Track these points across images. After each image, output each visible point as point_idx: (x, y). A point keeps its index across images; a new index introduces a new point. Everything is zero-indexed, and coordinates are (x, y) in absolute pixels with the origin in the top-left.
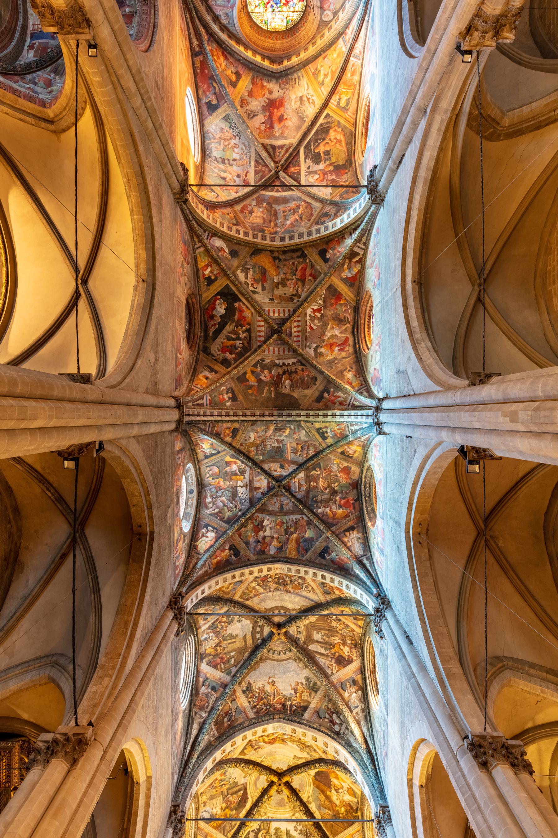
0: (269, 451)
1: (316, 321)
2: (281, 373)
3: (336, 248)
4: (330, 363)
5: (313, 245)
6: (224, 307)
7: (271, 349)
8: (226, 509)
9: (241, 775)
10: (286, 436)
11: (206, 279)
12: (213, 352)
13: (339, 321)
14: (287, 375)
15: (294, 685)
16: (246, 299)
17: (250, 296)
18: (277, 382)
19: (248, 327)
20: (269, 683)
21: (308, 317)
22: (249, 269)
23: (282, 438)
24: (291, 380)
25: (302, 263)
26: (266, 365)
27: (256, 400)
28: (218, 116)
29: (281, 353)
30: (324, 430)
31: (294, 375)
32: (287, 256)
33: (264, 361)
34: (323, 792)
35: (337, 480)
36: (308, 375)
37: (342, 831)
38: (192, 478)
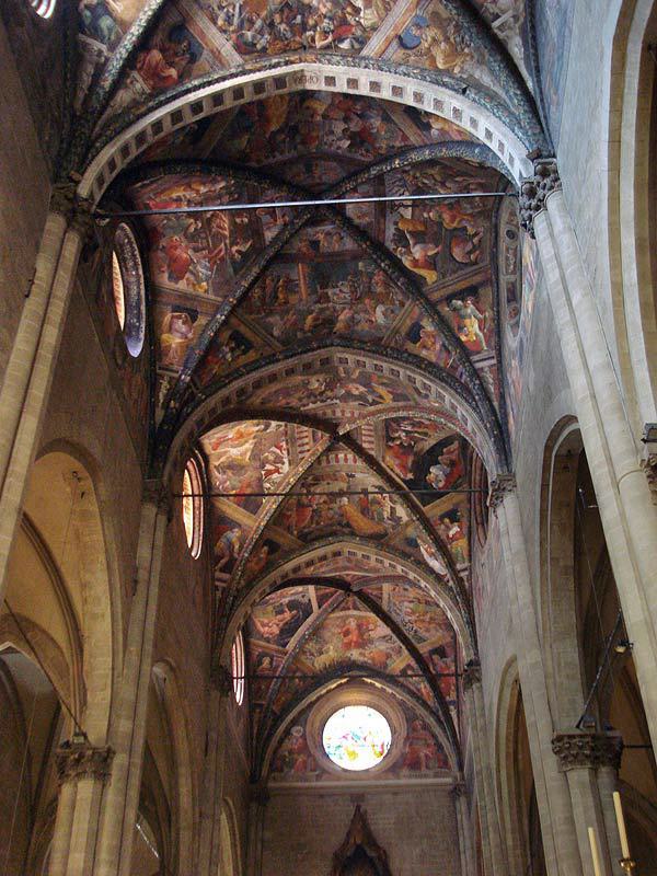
0: (344, 279)
1: (271, 458)
6: (431, 477)
8: (439, 178)
13: (233, 467)
19: (390, 443)
21: (286, 460)
28: (433, 643)
30: (238, 352)
32: (329, 530)
35: (192, 238)
38: (508, 265)
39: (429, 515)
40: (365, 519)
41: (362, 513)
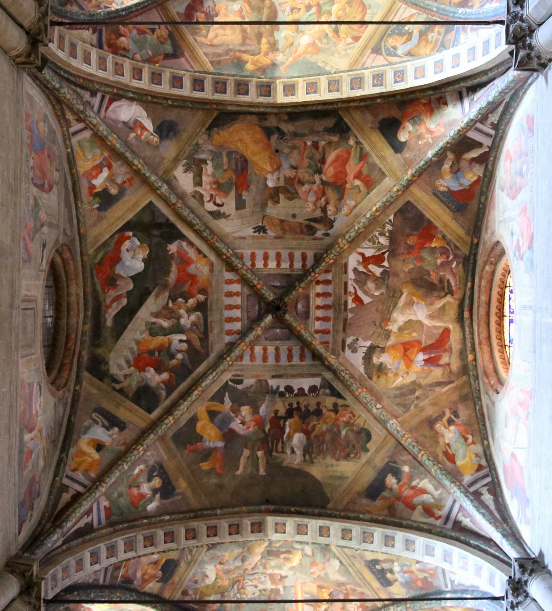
1: (371, 285)
2: (282, 412)
3: (421, 121)
4: (403, 395)
5: (367, 107)
6: (143, 254)
7: (258, 349)
10: (293, 568)
11: (98, 195)
12: (114, 370)
14: (296, 418)
16: (198, 233)
17: (208, 227)
18: (271, 437)
19: (201, 297)
21: (351, 275)
22: (204, 161)
23: (283, 573)
24: (307, 433)
25: (337, 145)
26: (244, 393)
27: (221, 487)
29: (284, 360)
30: (386, 566)
31: (314, 421)
33: (240, 382)
36: (347, 424)
39: (143, 190)
40: (241, 147)
41: (245, 161)
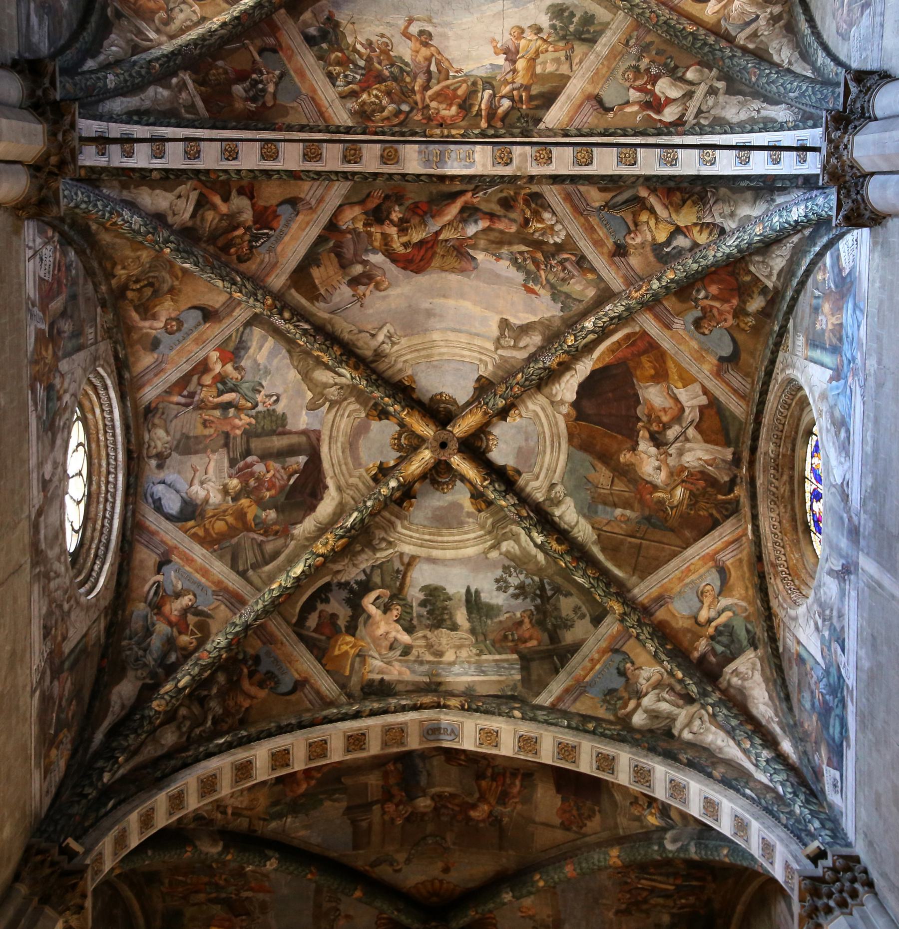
9: (300, 394)
15: (505, 39)
20: (406, 35)
34: (606, 458)
37: (674, 555)
